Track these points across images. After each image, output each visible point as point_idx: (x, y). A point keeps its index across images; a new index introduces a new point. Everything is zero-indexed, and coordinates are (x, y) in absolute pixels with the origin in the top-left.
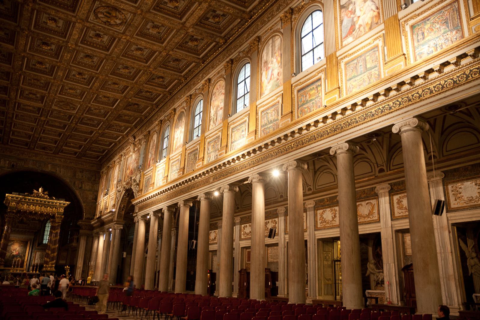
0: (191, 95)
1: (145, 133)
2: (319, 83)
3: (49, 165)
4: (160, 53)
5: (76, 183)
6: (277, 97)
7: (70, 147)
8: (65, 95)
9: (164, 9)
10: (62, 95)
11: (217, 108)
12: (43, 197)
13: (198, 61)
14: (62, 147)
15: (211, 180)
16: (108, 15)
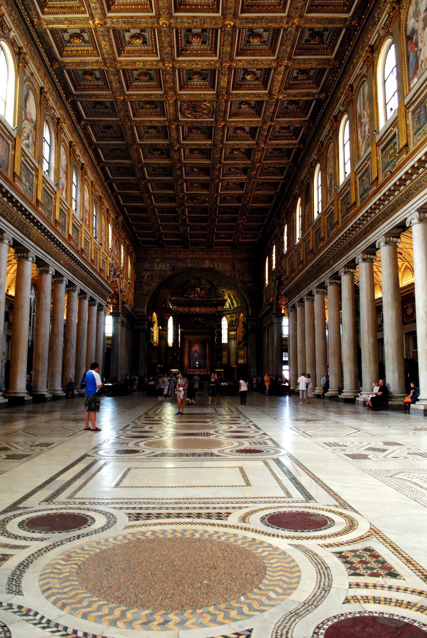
0: (311, 163)
1: (285, 212)
2: (394, 141)
3: (207, 261)
4: (261, 127)
5: (237, 276)
6: (368, 161)
7: (222, 238)
8: (192, 190)
9: (244, 85)
10: (190, 190)
11: (331, 178)
12: (201, 297)
13: (307, 123)
14: (213, 239)
15: (332, 263)
16: (194, 110)
